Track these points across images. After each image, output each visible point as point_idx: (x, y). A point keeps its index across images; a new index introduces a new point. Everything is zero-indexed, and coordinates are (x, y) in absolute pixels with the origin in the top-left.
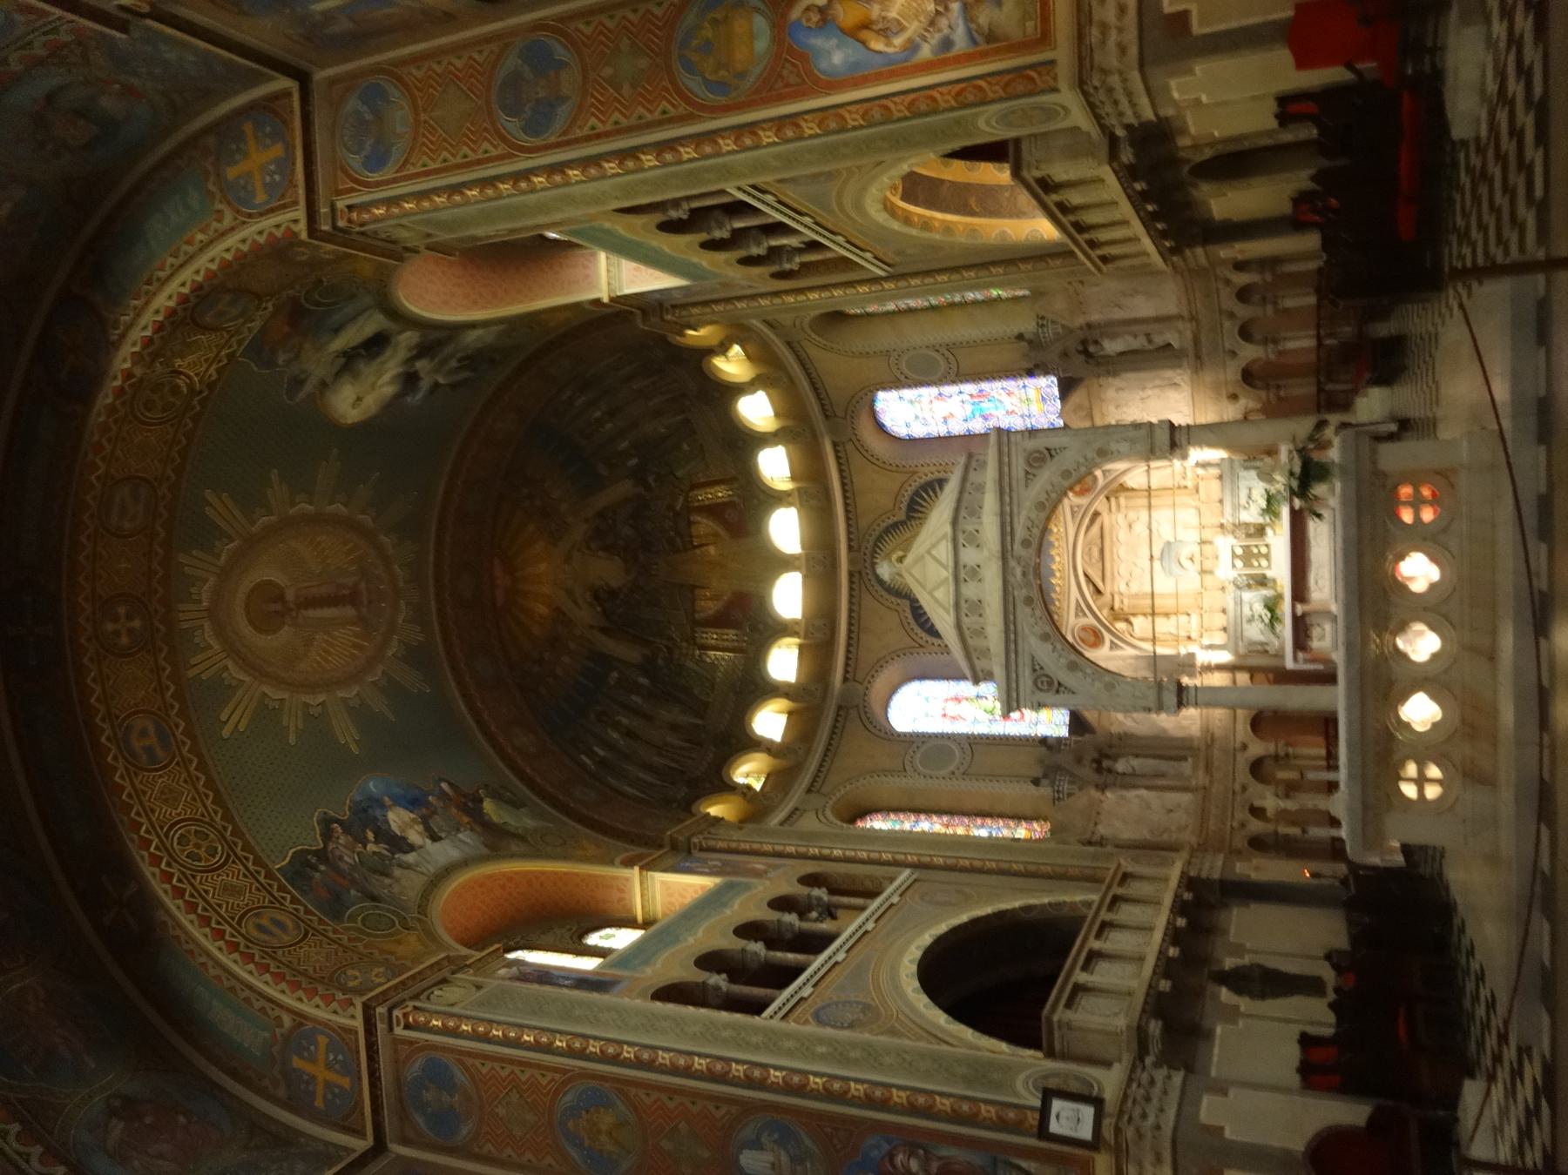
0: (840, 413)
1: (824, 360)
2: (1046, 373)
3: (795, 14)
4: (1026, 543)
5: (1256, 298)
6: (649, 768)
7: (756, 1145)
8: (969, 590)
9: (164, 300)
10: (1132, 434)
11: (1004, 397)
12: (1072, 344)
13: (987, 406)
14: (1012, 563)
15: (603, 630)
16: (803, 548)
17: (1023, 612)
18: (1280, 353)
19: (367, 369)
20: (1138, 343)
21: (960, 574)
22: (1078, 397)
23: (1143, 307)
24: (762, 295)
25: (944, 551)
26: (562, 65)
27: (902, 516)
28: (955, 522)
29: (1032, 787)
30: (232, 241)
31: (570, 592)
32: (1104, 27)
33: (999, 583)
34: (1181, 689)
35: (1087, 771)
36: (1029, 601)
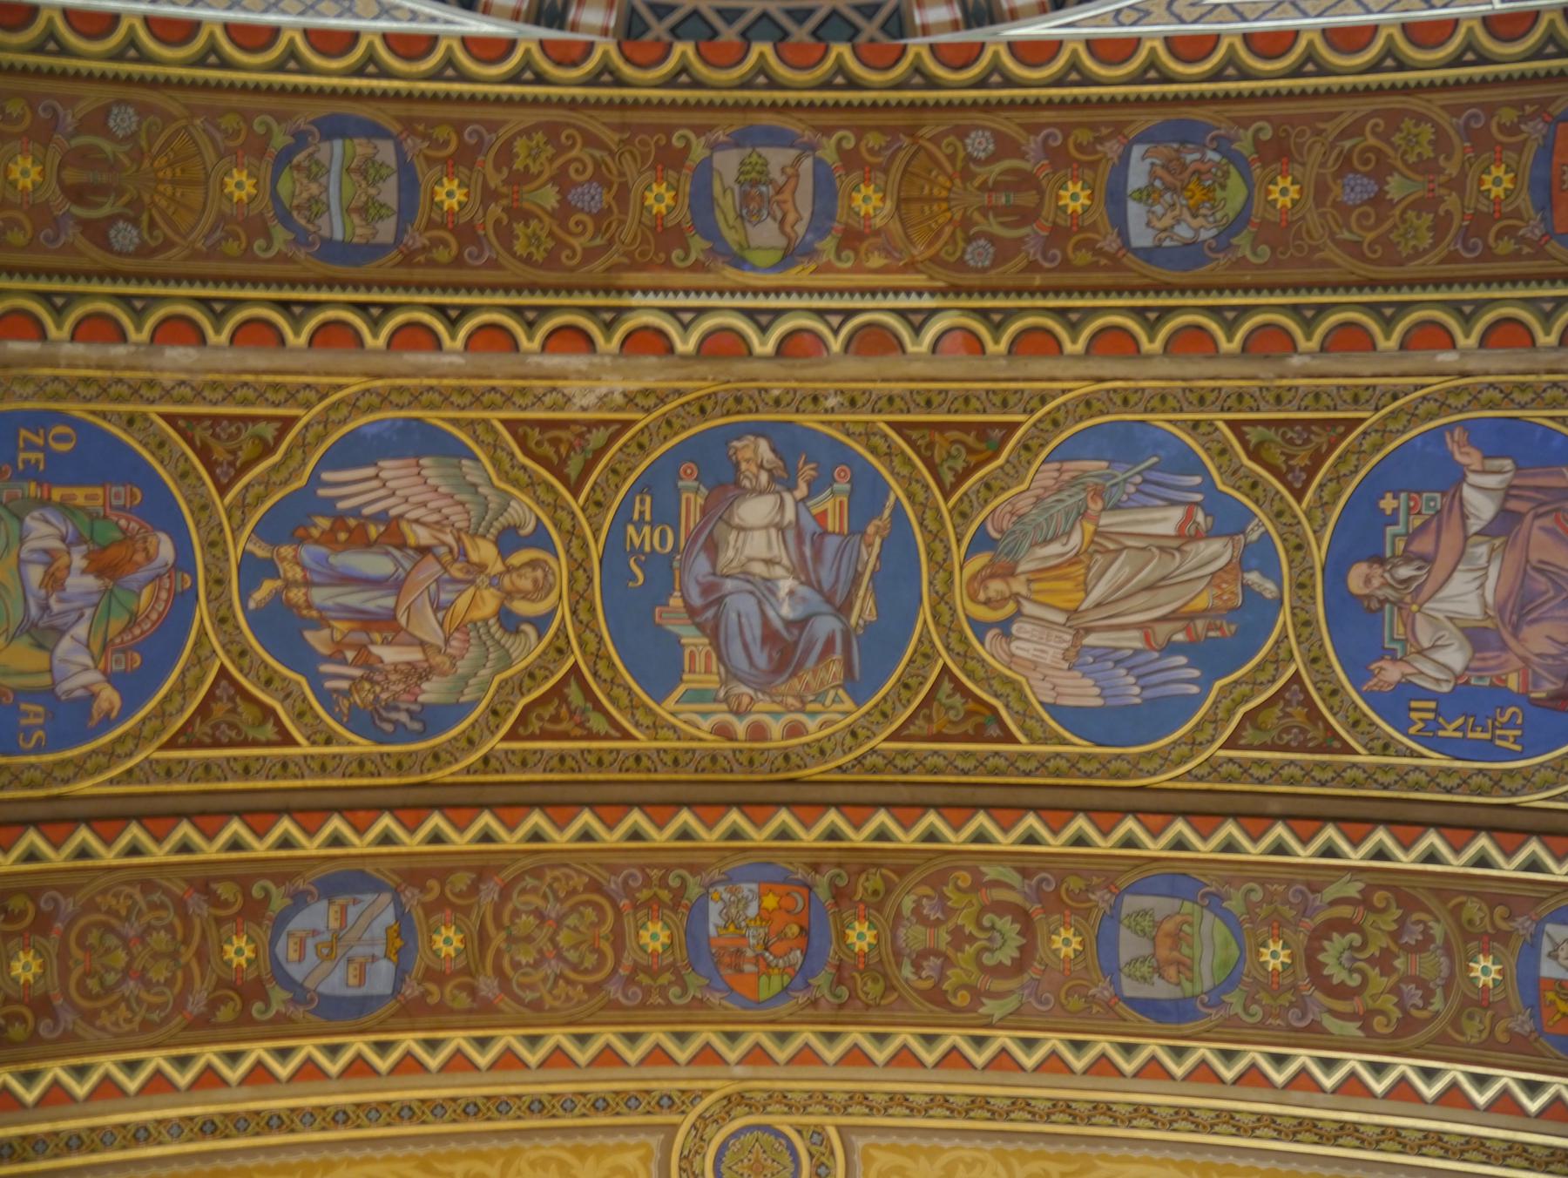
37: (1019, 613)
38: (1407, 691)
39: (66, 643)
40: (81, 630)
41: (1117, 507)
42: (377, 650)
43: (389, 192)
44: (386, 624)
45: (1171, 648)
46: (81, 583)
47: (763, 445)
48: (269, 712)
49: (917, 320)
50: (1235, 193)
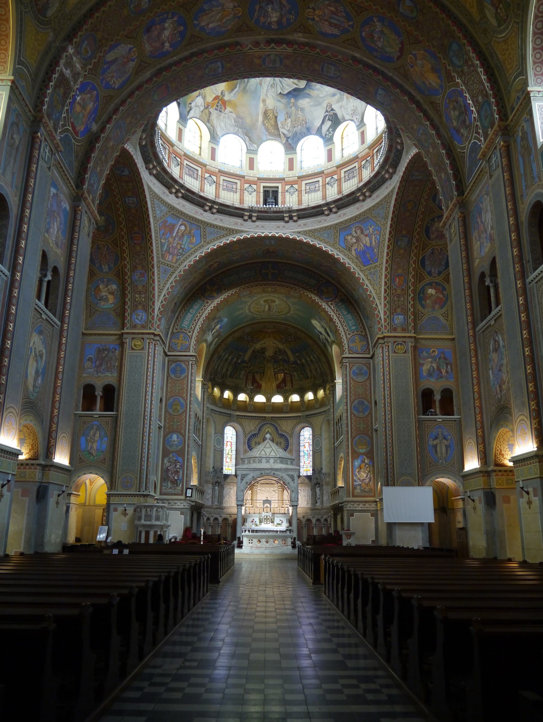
0: (308, 419)
1: (321, 418)
2: (313, 474)
3: (365, 457)
4: (274, 474)
5: (325, 523)
6: (218, 366)
7: (178, 438)
8: (264, 460)
9: (335, 317)
10: (296, 497)
11: (308, 462)
12: (319, 481)
13: (306, 457)
14: (270, 471)
15: (254, 351)
16: (273, 403)
17: (259, 473)
18: (313, 528)
19: (323, 329)
20: (318, 496)
21: (268, 459)
22: (307, 481)
23: (325, 498)
24: (334, 416)
25: (273, 454)
26: (364, 413)
27: (280, 432)
28: (280, 458)
29: (212, 467)
30: (344, 337)
31: (265, 343)
32: (353, 505)
33: (265, 468)
34: (242, 505)
35: (216, 480)
36: (261, 474)
37: (233, 9)
38: (172, 18)
39: (380, 29)
40: (377, 30)
41: (218, 26)
42: (335, 10)
43: (325, 69)
44: (332, 12)
45: (208, 10)
46: (376, 36)
47: (273, 27)
48: (353, 8)
49: (250, 49)
50: (207, 72)
